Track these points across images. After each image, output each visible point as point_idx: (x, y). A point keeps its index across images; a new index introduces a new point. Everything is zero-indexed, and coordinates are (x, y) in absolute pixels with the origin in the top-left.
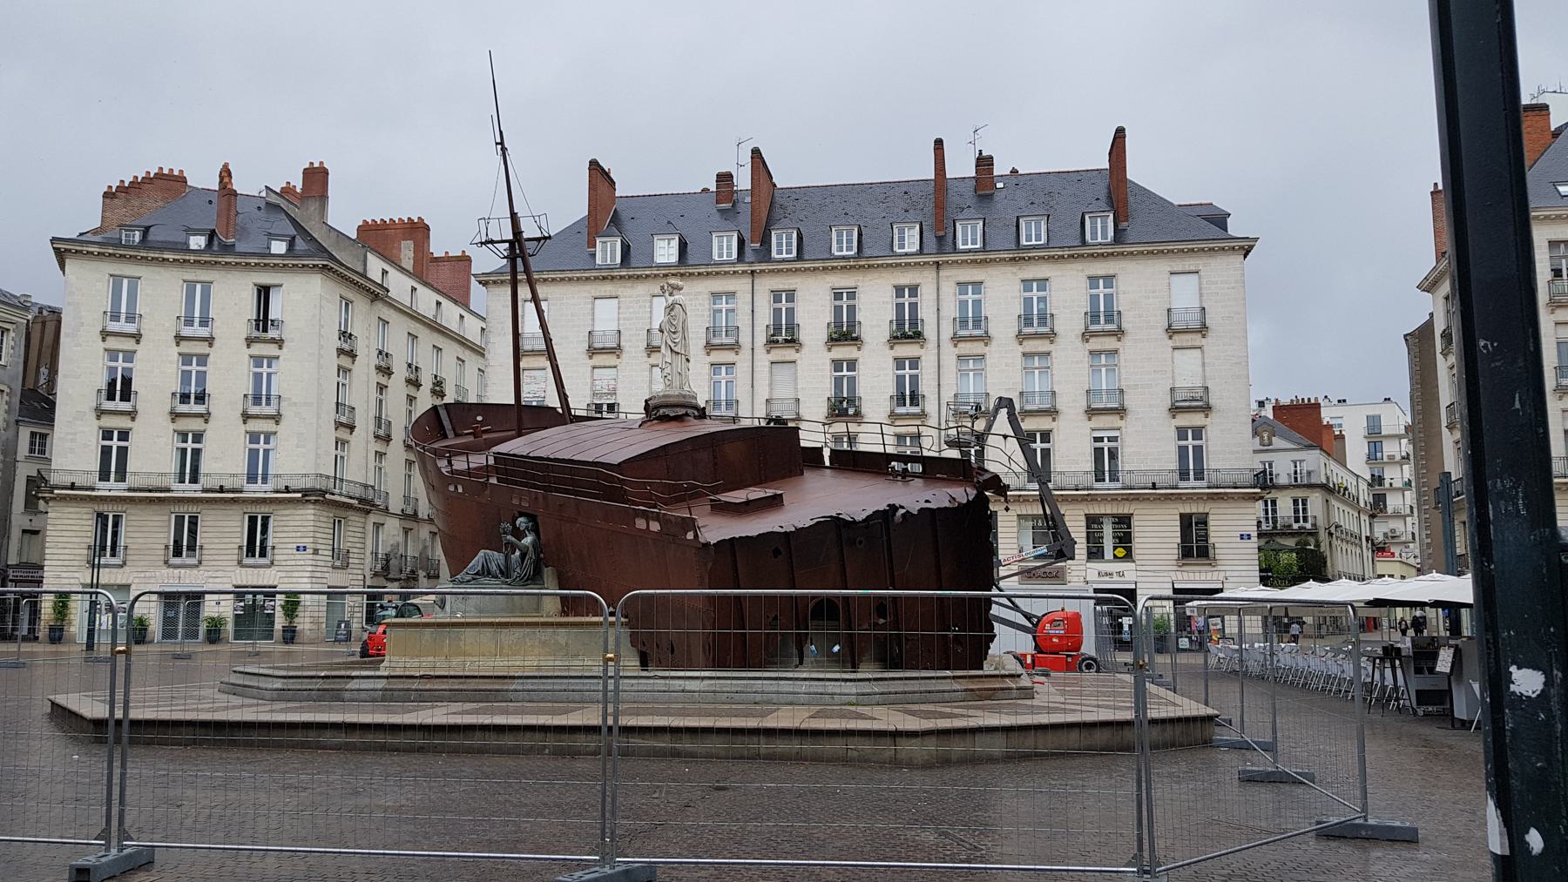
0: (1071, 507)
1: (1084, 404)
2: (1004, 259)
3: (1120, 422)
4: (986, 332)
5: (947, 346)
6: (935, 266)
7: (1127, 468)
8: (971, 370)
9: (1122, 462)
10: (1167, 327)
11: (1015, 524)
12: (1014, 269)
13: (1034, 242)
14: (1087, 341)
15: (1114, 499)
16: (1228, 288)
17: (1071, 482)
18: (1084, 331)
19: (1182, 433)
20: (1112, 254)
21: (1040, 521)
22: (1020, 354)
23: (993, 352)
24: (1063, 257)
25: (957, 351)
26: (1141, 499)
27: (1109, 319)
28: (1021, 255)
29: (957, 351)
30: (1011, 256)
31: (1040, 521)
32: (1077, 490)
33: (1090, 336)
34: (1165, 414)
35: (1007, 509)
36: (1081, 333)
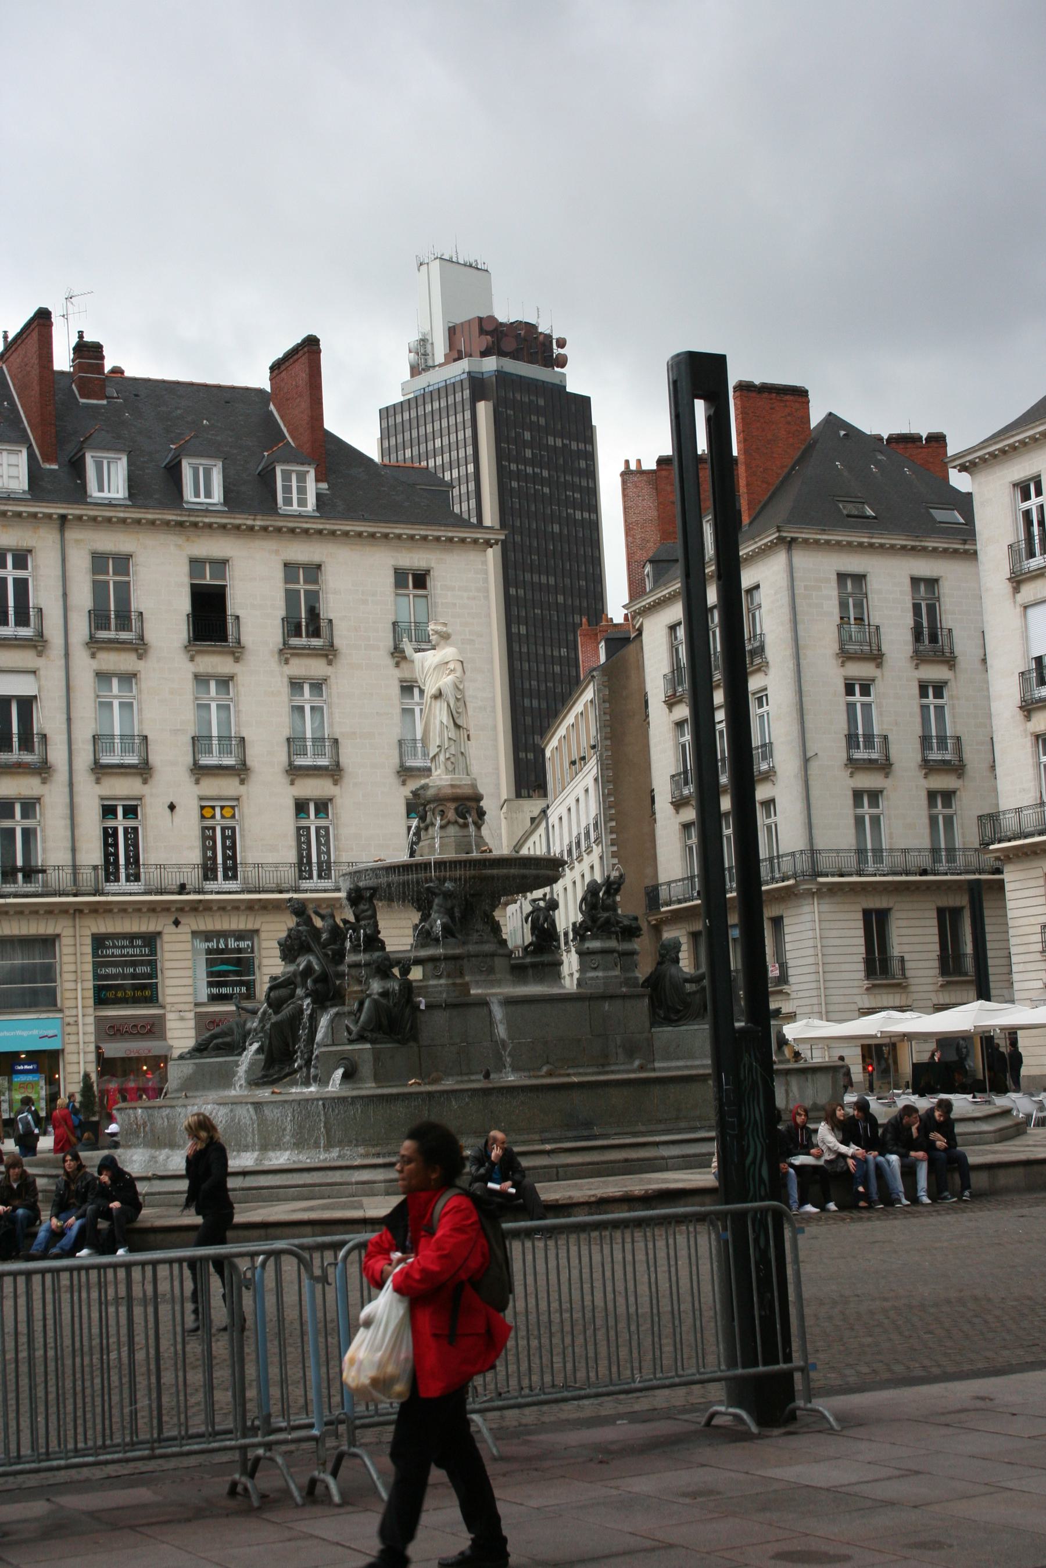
0: (269, 918)
1: (189, 760)
2: (167, 523)
3: (332, 787)
4: (142, 638)
5: (81, 657)
6: (56, 524)
7: (345, 857)
8: (116, 697)
9: (44, 850)
10: (392, 650)
11: (189, 946)
12: (180, 540)
13: (202, 499)
14: (287, 662)
15: (138, 909)
16: (468, 598)
17: (173, 880)
18: (281, 647)
19: (301, 807)
20: (320, 532)
21: (222, 941)
22: (190, 676)
23: (150, 670)
24: (251, 528)
25: (94, 665)
26: (101, 910)
27: (316, 633)
28: (192, 519)
29: (94, 665)
30: (179, 518)
31: (222, 941)
32: (281, 892)
33: (293, 655)
34: (393, 780)
35: (177, 923)
36: (276, 650)
